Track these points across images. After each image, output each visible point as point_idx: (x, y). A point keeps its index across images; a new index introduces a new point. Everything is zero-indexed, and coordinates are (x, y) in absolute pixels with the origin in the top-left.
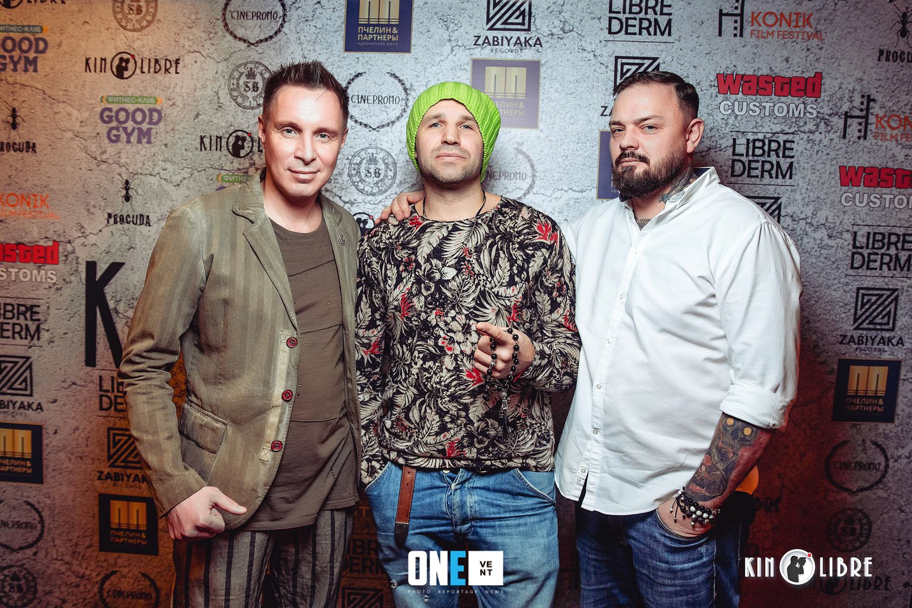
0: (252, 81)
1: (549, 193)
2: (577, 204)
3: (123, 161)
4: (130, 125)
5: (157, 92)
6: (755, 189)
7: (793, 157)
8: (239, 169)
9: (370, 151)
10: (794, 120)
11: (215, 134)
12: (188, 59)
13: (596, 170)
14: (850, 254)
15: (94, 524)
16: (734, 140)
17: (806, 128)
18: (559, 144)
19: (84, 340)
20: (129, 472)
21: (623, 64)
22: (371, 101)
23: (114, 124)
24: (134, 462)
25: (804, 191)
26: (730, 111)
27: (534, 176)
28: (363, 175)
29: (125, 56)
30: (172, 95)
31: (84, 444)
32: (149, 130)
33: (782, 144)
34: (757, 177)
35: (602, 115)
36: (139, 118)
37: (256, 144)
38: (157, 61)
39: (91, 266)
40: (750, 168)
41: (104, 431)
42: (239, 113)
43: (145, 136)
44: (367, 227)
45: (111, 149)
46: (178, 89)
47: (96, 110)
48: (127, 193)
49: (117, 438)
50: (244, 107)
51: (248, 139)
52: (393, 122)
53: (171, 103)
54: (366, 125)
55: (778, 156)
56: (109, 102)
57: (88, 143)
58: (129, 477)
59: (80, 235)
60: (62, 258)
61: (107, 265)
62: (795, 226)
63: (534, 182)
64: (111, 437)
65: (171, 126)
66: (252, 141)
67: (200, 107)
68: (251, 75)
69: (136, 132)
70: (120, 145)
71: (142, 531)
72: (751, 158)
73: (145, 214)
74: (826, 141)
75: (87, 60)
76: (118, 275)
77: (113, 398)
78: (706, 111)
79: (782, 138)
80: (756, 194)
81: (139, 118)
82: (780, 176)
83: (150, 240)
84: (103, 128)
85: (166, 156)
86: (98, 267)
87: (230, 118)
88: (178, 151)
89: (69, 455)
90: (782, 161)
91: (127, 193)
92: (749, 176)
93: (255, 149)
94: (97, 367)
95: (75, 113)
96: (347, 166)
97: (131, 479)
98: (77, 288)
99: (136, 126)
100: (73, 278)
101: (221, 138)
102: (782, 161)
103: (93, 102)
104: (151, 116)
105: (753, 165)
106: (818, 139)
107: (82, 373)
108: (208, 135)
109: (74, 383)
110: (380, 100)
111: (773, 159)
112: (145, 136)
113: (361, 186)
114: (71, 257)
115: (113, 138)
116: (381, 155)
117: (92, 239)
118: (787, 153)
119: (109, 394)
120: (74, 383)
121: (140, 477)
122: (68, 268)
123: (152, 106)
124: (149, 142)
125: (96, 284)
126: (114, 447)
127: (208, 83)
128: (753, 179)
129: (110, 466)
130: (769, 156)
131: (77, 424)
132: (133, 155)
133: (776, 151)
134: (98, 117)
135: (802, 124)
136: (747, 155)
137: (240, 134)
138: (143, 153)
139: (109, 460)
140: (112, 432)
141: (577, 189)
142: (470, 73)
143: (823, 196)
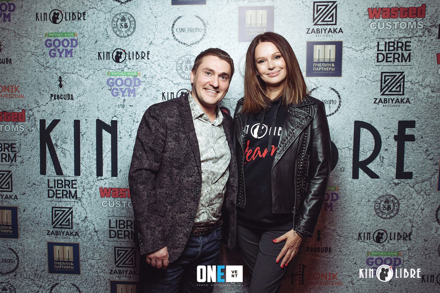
3: (57, 67)
4: (61, 48)
5: (75, 30)
6: (390, 68)
7: (410, 50)
8: (119, 69)
9: (187, 57)
10: (411, 30)
11: (106, 51)
15: (45, 259)
16: (378, 43)
20: (63, 230)
22: (187, 31)
23: (53, 48)
24: (67, 225)
26: (375, 28)
28: (184, 69)
30: (83, 31)
32: (71, 50)
33: (404, 44)
34: (391, 61)
35: (307, 33)
36: (66, 44)
39: (43, 122)
40: (387, 57)
42: (119, 40)
43: (69, 53)
45: (51, 61)
46: (85, 28)
47: (43, 40)
48: (61, 83)
49: (57, 212)
50: (121, 37)
52: (199, 42)
53: (82, 36)
54: (184, 44)
55: (402, 50)
56: (50, 36)
57: (39, 58)
58: (63, 233)
60: (27, 119)
61: (51, 121)
62: (413, 87)
64: (54, 212)
65: (83, 48)
66: (126, 54)
67: (98, 37)
71: (71, 262)
72: (387, 52)
73: (70, 94)
76: (57, 126)
77: (55, 191)
78: (362, 28)
79: (404, 41)
80: (391, 71)
82: (404, 61)
83: (73, 107)
84: (47, 50)
85: (81, 63)
87: (113, 42)
88: (87, 60)
89: (31, 223)
90: (404, 52)
91: (61, 83)
92: (387, 61)
93: (127, 58)
95: (32, 43)
97: (64, 234)
98: (36, 134)
99: (64, 48)
100: (33, 129)
101: (109, 53)
102: (404, 52)
103: (41, 36)
104: (72, 43)
105: (389, 56)
108: (102, 52)
109: (34, 184)
110: (191, 30)
111: (400, 51)
112: (69, 53)
113: (183, 75)
115: (53, 55)
117: (43, 108)
118: (407, 48)
119: (53, 189)
120: (34, 184)
122: (30, 123)
123: (72, 38)
124: (71, 56)
128: (389, 63)
130: (397, 50)
131: (35, 206)
132: (63, 63)
133: (401, 48)
134: (44, 44)
136: (385, 50)
137: (119, 50)
138: (68, 62)
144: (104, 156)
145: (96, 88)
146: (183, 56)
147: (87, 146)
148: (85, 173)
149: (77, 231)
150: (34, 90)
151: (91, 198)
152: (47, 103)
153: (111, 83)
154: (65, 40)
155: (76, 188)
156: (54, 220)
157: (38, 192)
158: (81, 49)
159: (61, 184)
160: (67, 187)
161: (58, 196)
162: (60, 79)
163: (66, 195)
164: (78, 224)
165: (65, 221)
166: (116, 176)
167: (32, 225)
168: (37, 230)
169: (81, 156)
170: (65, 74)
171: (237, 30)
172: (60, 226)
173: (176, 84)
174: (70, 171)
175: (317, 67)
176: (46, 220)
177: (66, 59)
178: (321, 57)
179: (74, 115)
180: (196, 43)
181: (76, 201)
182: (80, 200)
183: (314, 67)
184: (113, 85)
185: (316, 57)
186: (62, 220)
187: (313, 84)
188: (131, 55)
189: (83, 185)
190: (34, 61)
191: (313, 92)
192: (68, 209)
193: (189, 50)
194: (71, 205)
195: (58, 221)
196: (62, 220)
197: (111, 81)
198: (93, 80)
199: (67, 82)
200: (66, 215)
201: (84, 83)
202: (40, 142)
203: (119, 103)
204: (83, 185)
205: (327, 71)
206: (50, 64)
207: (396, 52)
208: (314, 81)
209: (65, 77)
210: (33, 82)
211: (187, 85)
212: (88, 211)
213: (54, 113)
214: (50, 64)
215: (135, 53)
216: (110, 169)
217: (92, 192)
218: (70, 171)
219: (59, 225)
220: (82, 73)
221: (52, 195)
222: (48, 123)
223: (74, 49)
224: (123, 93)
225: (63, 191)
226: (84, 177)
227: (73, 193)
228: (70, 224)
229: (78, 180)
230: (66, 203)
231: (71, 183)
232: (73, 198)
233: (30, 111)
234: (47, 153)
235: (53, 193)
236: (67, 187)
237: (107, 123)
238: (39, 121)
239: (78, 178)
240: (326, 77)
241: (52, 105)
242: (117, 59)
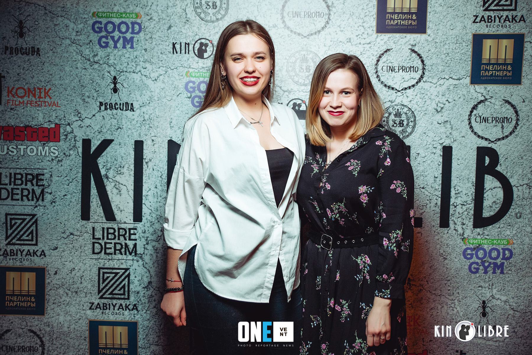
1: (434, 81)
2: (456, 89)
4: (116, 34)
8: (203, 68)
9: (303, 53)
11: (184, 41)
13: (470, 63)
18: (442, 44)
19: (80, 200)
20: (114, 302)
23: (104, 34)
27: (424, 69)
28: (297, 70)
31: (79, 282)
32: (132, 38)
39: (87, 143)
41: (95, 270)
43: (129, 42)
44: (301, 109)
45: (102, 53)
48: (115, 86)
51: (210, 45)
54: (299, 34)
58: (114, 306)
59: (78, 119)
60: (62, 137)
61: (100, 142)
63: (424, 73)
64: (101, 275)
65: (149, 35)
69: (122, 39)
70: (109, 50)
73: (130, 102)
77: (103, 244)
83: (133, 122)
84: (94, 37)
85: (146, 58)
86: (92, 143)
88: (155, 54)
91: (115, 86)
94: (91, 221)
96: (286, 64)
97: (116, 308)
98: (75, 160)
99: (121, 35)
100: (71, 152)
101: (188, 44)
107: (79, 226)
108: (178, 42)
109: (72, 234)
112: (129, 42)
113: (296, 79)
114: (70, 136)
115: (103, 45)
116: (311, 56)
117: (87, 122)
119: (100, 241)
120: (72, 234)
121: (124, 306)
122: (68, 144)
124: (132, 47)
126: (103, 283)
129: (99, 298)
131: (73, 266)
132: (119, 57)
137: (203, 41)
138: (127, 55)
139: (98, 294)
140: (102, 271)
141: (456, 78)
145: (169, 94)
146: (297, 52)
147: (153, 179)
148: (149, 218)
149: (136, 302)
150: (74, 95)
151: (158, 255)
152: (94, 115)
153: (191, 87)
155: (136, 240)
156: (101, 287)
157: (77, 245)
158: (147, 37)
159: (114, 234)
160: (122, 238)
161: (108, 251)
163: (120, 250)
164: (138, 293)
165: (118, 288)
167: (67, 294)
168: (74, 302)
169: (144, 193)
170: (122, 74)
172: (110, 296)
173: (286, 91)
174: (127, 215)
175: (486, 70)
176: (89, 287)
177: (124, 51)
178: (494, 56)
179: (135, 134)
180: (316, 33)
181: (135, 258)
183: (483, 70)
184: (194, 91)
185: (486, 55)
186: (114, 287)
187: (480, 95)
190: (75, 53)
191: (479, 106)
192: (123, 271)
193: (305, 43)
194: (128, 264)
195: (107, 288)
196: (114, 287)
198: (163, 82)
200: (120, 280)
201: (150, 87)
202: (82, 173)
204: (146, 235)
205: (500, 76)
206: (99, 58)
208: (482, 91)
209: (123, 77)
210: (73, 84)
211: (301, 93)
213: (105, 130)
214: (99, 58)
219: (109, 294)
220: (148, 72)
221: (99, 251)
222: (95, 144)
223: (136, 37)
225: (115, 244)
226: (148, 224)
227: (131, 247)
228: (126, 293)
229: (138, 229)
232: (130, 254)
233: (68, 127)
234: (92, 189)
235: (99, 247)
236: (122, 238)
238: (81, 141)
239: (139, 225)
240: (498, 85)
241: (101, 118)
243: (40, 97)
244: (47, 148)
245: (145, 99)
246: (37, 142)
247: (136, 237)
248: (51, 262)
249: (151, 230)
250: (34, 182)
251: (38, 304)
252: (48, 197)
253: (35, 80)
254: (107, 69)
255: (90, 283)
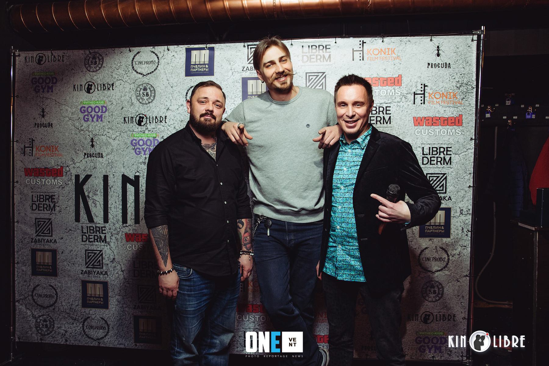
0: (145, 92)
4: (93, 113)
12: (117, 83)
14: (421, 158)
15: (80, 295)
17: (396, 101)
20: (95, 270)
21: (309, 76)
23: (86, 113)
25: (397, 129)
29: (90, 83)
32: (102, 115)
36: (97, 111)
37: (148, 120)
38: (104, 85)
39: (77, 177)
41: (84, 251)
43: (100, 118)
45: (85, 124)
46: (114, 97)
49: (90, 254)
50: (143, 104)
51: (145, 117)
60: (64, 174)
65: (111, 113)
68: (145, 89)
70: (89, 123)
71: (101, 298)
73: (101, 153)
74: (406, 106)
75: (74, 86)
81: (97, 111)
82: (385, 123)
84: (81, 116)
87: (137, 109)
93: (148, 122)
95: (69, 109)
98: (71, 186)
102: (386, 116)
106: (402, 105)
109: (70, 230)
111: (381, 115)
112: (100, 118)
117: (78, 165)
118: (388, 112)
120: (70, 230)
124: (102, 121)
125: (80, 184)
127: (127, 94)
132: (95, 126)
133: (382, 111)
135: (394, 98)
137: (141, 115)
138: (99, 125)
142: (241, 84)
143: (406, 131)
144: (128, 206)
154: (97, 107)
159: (93, 230)
161: (91, 240)
162: (92, 140)
163: (97, 240)
166: (139, 223)
171: (241, 97)
174: (100, 219)
177: (97, 123)
182: (109, 244)
184: (136, 145)
188: (151, 119)
189: (111, 231)
197: (134, 141)
199: (98, 143)
203: (141, 161)
204: (111, 231)
207: (378, 115)
212: (115, 254)
215: (154, 118)
216: (134, 217)
217: (118, 237)
218: (100, 219)
222: (82, 177)
223: (104, 115)
224: (145, 151)
227: (103, 237)
228: (101, 264)
230: (98, 246)
231: (101, 230)
236: (98, 233)
237: (131, 178)
239: (107, 225)
242: (139, 124)
243: (53, 151)
244: (56, 180)
245: (109, 150)
246: (51, 177)
247: (106, 232)
248: (60, 246)
249: (114, 228)
250: (50, 200)
251: (52, 270)
252: (57, 209)
253: (50, 141)
254: (88, 134)
255: (81, 260)
